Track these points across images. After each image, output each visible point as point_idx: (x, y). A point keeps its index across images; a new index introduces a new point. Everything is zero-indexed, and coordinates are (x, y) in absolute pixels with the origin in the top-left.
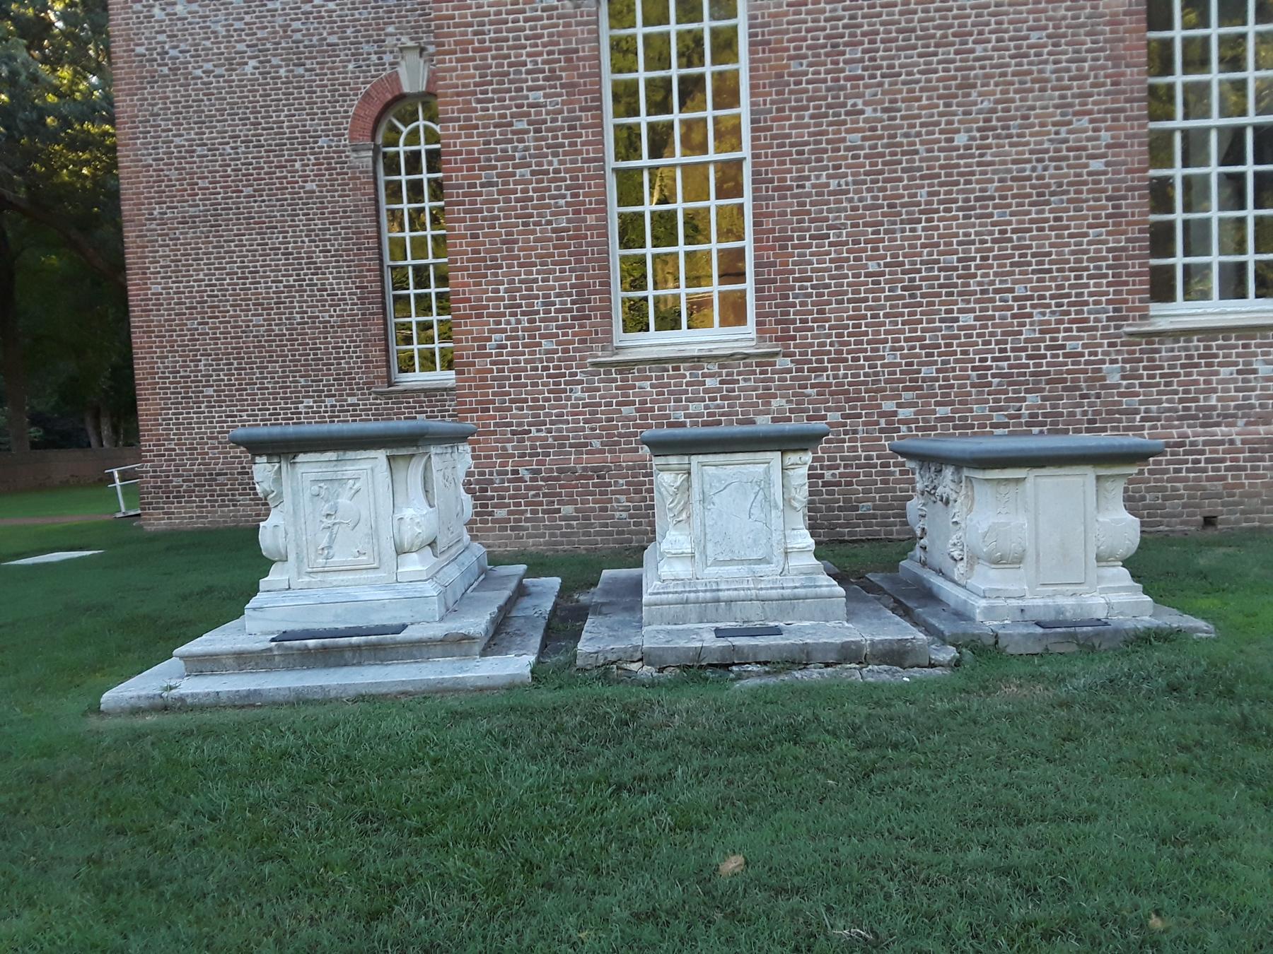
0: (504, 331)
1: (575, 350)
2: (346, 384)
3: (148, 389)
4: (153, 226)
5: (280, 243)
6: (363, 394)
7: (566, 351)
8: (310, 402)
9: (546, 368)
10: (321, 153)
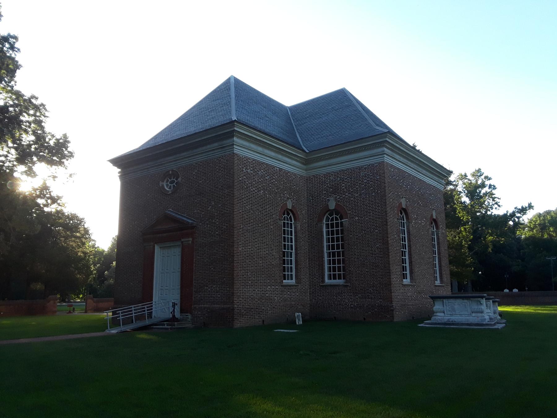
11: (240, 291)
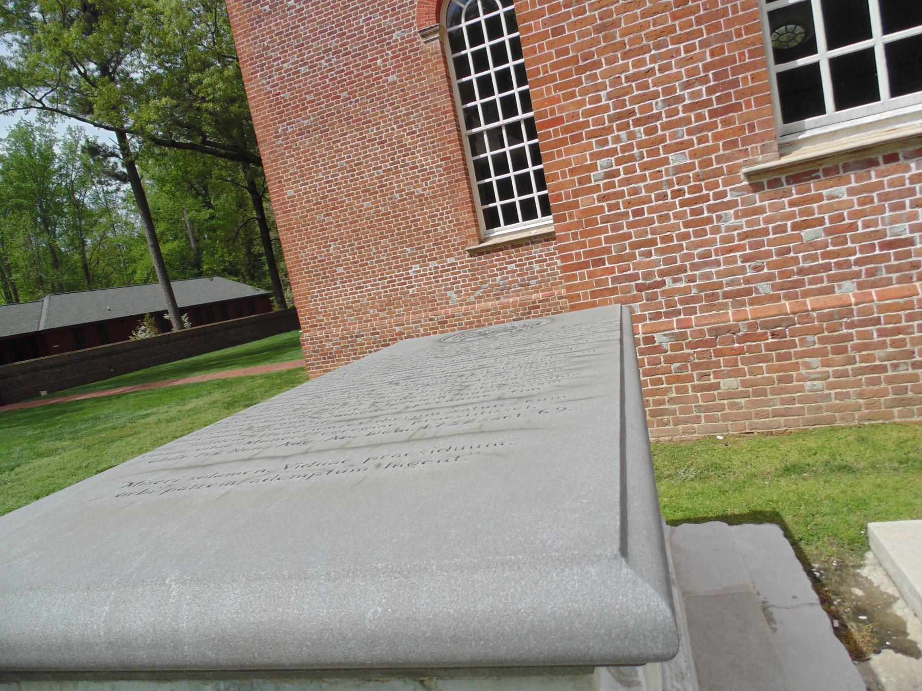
0: (613, 152)
1: (719, 159)
2: (444, 247)
3: (297, 275)
4: (280, 142)
5: (375, 134)
6: (459, 254)
7: (706, 163)
8: (416, 267)
9: (677, 193)
10: (396, 46)
11: (312, 297)
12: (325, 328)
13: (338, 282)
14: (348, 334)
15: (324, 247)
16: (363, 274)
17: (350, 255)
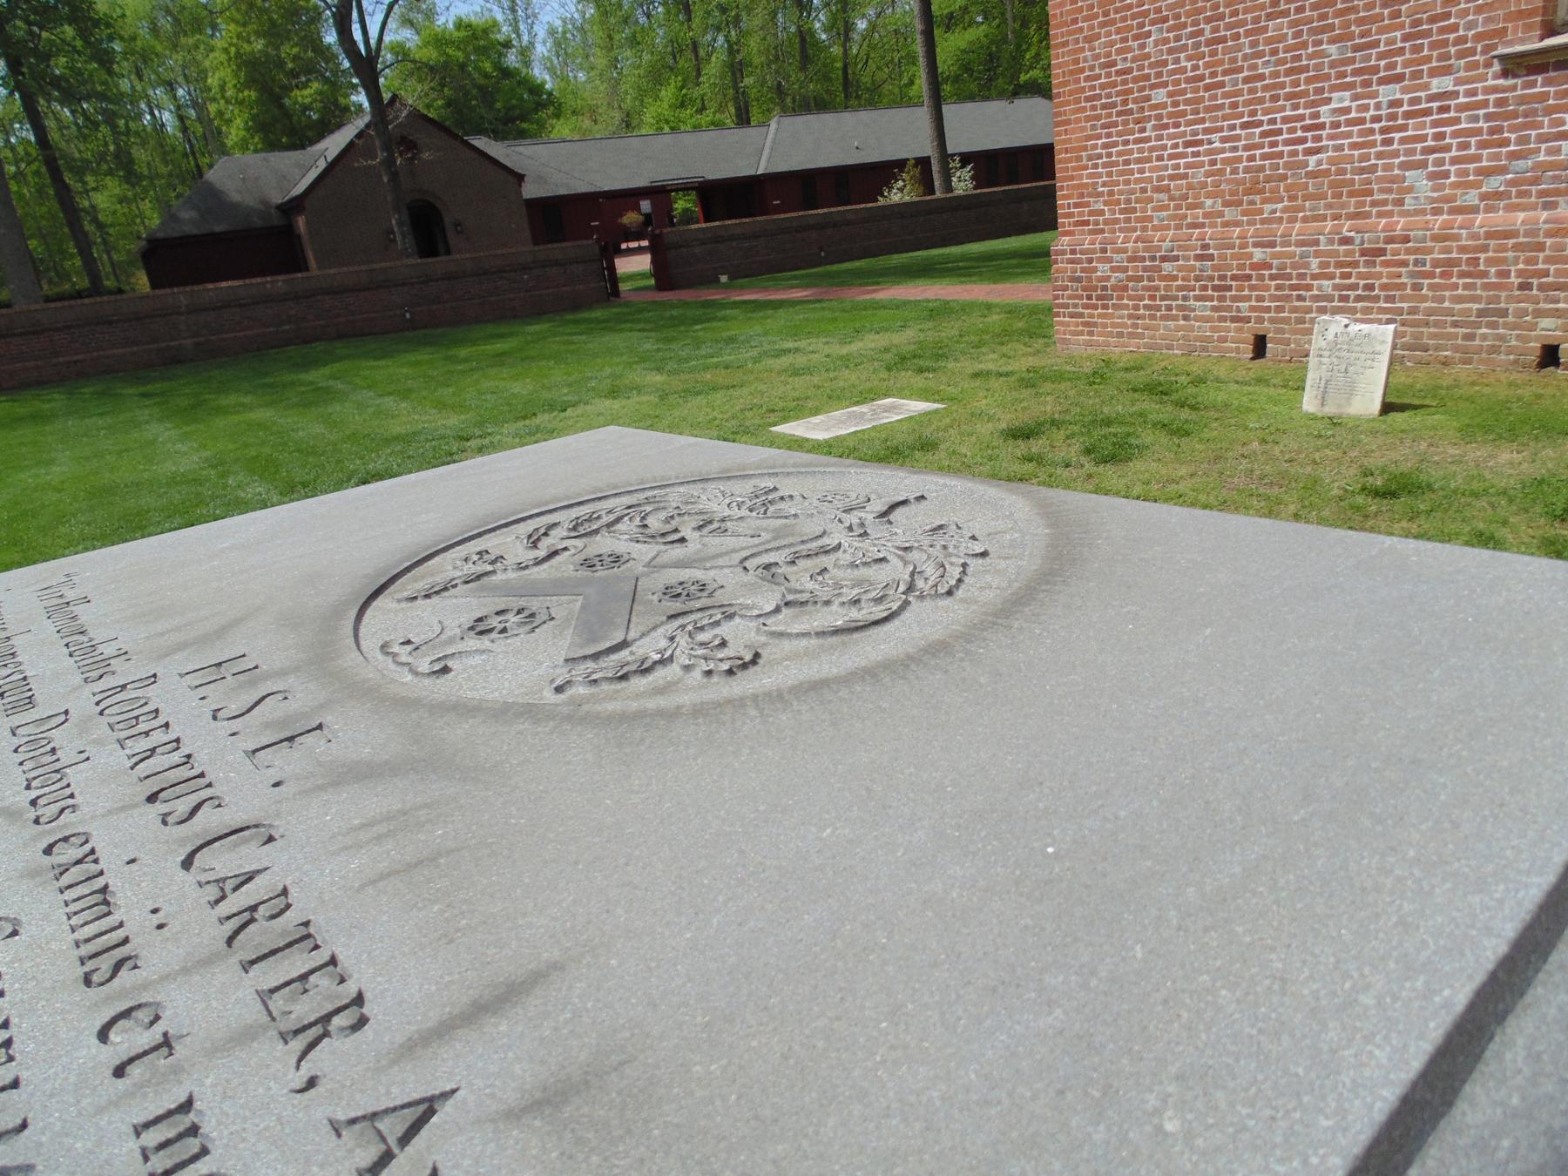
3: (1068, 103)
8: (1342, 99)
11: (1090, 158)
12: (1102, 231)
13: (1149, 126)
14: (1146, 250)
15: (1136, 38)
16: (1209, 109)
17: (1189, 59)
